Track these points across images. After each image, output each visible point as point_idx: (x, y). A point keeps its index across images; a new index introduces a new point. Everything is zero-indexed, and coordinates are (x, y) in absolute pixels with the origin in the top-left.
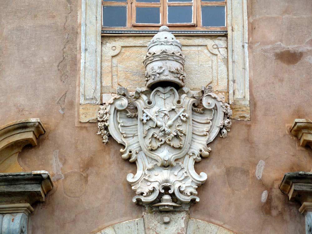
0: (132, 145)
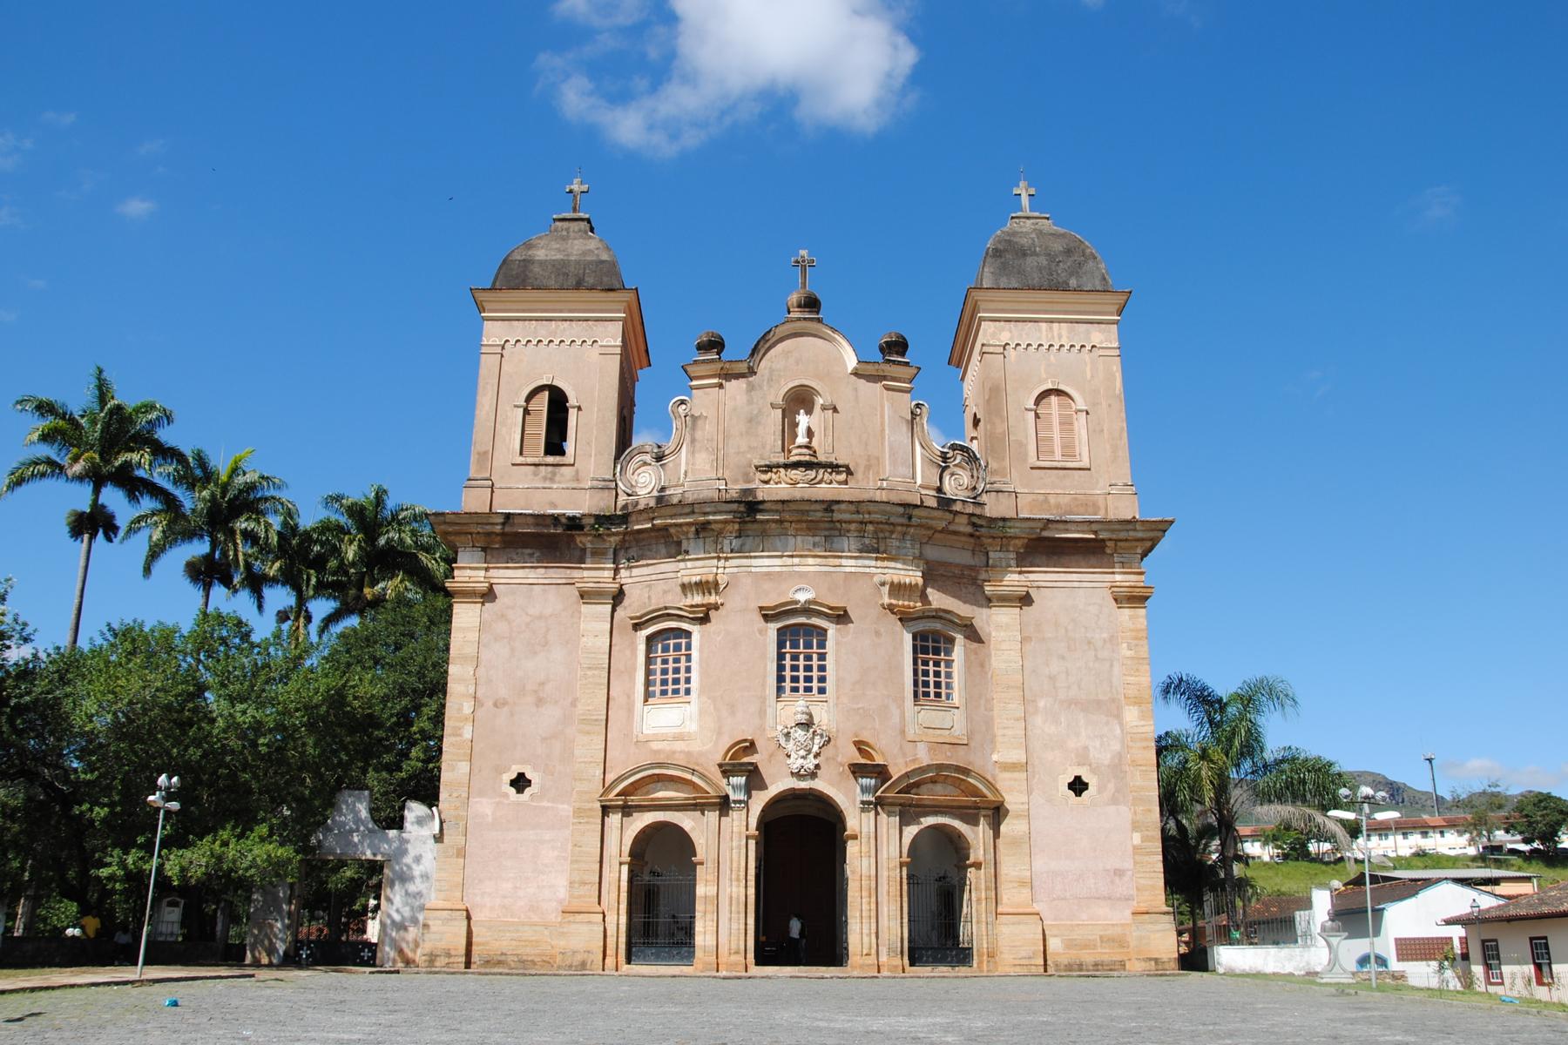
0: (790, 746)
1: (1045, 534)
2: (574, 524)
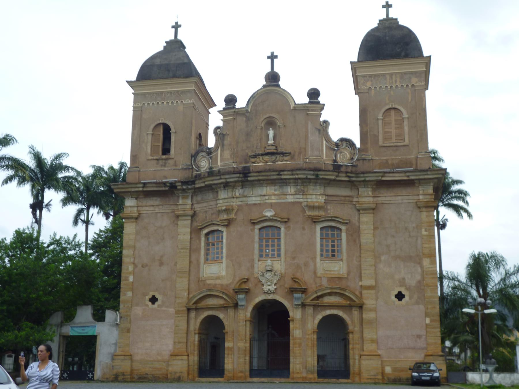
0: (263, 281)
1: (384, 179)
2: (173, 186)
